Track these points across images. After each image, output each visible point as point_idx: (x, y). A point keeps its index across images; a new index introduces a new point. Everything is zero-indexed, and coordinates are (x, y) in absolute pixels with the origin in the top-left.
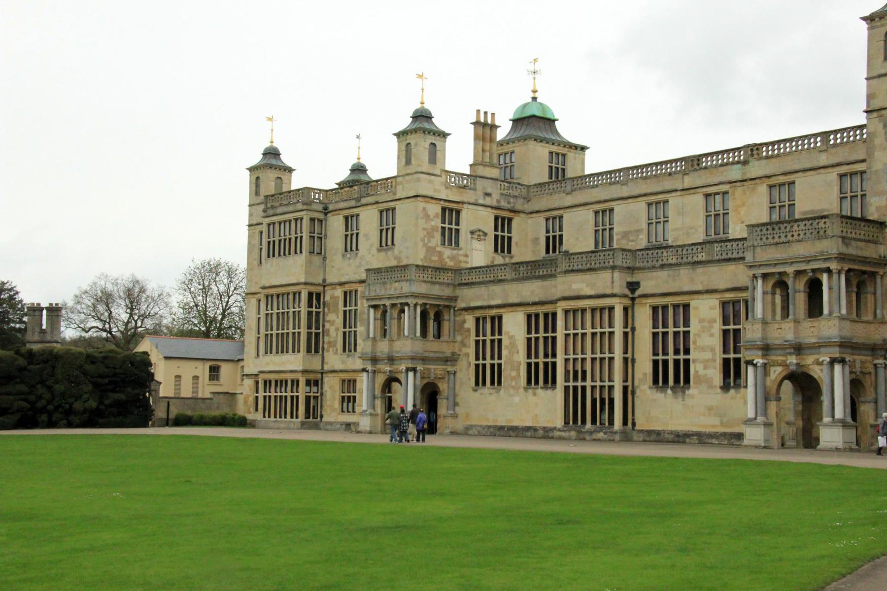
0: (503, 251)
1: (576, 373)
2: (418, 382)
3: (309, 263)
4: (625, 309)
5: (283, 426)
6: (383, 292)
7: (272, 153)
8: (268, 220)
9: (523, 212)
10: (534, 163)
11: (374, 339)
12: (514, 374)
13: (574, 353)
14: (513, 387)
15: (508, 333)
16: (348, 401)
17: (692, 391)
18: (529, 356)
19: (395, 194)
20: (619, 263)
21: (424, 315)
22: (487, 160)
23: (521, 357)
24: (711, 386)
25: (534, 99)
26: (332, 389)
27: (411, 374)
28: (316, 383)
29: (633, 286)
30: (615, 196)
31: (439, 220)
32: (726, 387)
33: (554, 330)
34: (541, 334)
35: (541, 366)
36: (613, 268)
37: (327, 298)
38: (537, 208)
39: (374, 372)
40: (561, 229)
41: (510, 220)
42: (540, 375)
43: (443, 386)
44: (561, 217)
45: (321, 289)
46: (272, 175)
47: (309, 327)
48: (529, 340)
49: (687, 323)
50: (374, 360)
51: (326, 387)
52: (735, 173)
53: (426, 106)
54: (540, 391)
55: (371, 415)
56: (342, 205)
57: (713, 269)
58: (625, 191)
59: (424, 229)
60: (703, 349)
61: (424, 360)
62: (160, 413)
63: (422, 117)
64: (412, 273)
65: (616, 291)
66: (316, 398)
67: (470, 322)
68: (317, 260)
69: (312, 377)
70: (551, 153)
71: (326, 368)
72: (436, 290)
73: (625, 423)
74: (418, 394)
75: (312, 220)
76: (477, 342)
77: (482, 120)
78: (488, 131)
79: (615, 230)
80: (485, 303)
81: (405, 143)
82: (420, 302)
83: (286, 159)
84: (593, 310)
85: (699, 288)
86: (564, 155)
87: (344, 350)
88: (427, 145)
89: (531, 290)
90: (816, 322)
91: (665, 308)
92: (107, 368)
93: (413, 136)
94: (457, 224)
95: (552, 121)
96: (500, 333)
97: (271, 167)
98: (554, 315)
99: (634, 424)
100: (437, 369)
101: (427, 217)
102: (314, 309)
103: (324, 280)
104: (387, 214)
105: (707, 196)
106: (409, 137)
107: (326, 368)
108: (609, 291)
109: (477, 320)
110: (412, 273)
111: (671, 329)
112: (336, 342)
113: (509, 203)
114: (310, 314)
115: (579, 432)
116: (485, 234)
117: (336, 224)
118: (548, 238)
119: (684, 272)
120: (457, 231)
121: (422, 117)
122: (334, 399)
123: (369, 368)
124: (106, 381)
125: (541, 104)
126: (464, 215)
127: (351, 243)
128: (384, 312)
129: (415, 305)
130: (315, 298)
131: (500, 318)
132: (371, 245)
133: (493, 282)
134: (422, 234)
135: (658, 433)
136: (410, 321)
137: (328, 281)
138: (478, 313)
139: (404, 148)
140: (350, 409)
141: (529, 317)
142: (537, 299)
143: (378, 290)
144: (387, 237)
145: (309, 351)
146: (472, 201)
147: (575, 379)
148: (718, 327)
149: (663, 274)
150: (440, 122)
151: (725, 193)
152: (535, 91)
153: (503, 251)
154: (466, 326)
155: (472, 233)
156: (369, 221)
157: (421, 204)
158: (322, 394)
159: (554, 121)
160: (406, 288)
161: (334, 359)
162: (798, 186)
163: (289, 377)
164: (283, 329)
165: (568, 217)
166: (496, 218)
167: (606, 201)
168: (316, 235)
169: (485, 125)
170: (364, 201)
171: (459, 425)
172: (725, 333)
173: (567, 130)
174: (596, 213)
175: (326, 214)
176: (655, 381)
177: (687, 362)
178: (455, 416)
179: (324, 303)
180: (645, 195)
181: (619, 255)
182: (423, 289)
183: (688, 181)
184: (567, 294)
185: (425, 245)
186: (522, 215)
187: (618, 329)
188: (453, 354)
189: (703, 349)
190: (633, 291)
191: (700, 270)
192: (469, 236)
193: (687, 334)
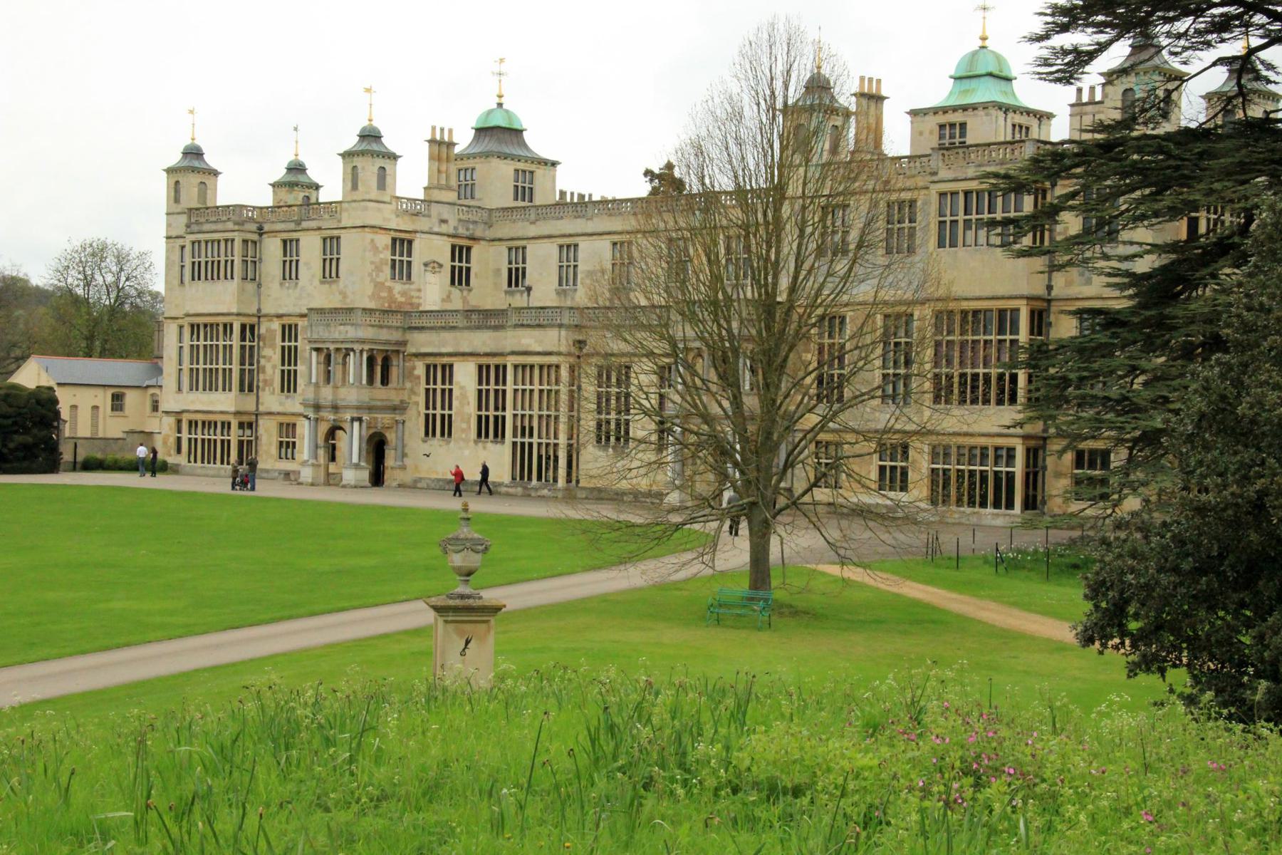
0: (460, 283)
1: (523, 428)
2: (364, 432)
3: (242, 291)
4: (572, 369)
5: (212, 472)
6: (325, 335)
7: (193, 153)
8: (193, 237)
9: (483, 239)
10: (496, 184)
11: (317, 385)
12: (464, 426)
13: (523, 409)
14: (463, 440)
15: (458, 383)
16: (287, 447)
18: (480, 409)
19: (340, 221)
20: (566, 321)
21: (371, 361)
22: (443, 182)
23: (472, 409)
25: (500, 105)
26: (268, 434)
27: (356, 424)
28: (250, 425)
29: (580, 344)
30: (579, 231)
31: (389, 252)
33: (504, 383)
35: (491, 420)
36: (560, 326)
37: (263, 331)
38: (499, 235)
39: (317, 420)
40: (524, 262)
41: (469, 249)
42: (489, 428)
43: (391, 436)
44: (524, 248)
45: (255, 320)
46: (195, 179)
47: (242, 363)
48: (480, 391)
50: (317, 407)
51: (261, 431)
53: (375, 124)
54: (490, 445)
55: (313, 465)
58: (590, 227)
59: (372, 263)
61: (371, 409)
62: (67, 456)
63: (370, 135)
64: (358, 317)
65: (563, 349)
66: (249, 442)
67: (420, 370)
68: (250, 287)
69: (245, 419)
70: (517, 171)
71: (262, 409)
72: (384, 335)
73: (569, 481)
74: (364, 445)
75: (245, 242)
76: (427, 390)
77: (438, 138)
78: (444, 149)
79: (580, 269)
80: (435, 350)
81: (351, 166)
82: (367, 347)
83: (211, 160)
84: (541, 367)
86: (532, 172)
87: (282, 391)
88: (375, 169)
89: (482, 341)
92: (11, 406)
93: (360, 158)
94: (410, 255)
96: (451, 383)
97: (194, 170)
98: (505, 367)
99: (578, 482)
100: (384, 419)
101: (375, 249)
102: (247, 343)
103: (259, 310)
104: (331, 244)
106: (355, 159)
107: (262, 409)
108: (555, 349)
109: (428, 367)
110: (358, 317)
112: (272, 380)
113: (468, 229)
114: (243, 347)
115: (525, 488)
116: (441, 266)
117: (272, 249)
118: (510, 270)
120: (409, 263)
121: (370, 135)
122: (271, 444)
123: (312, 415)
124: (10, 421)
125: (507, 111)
126: (416, 245)
127: (290, 270)
128: (328, 357)
129: (361, 351)
130: (249, 331)
131: (451, 366)
132: (313, 276)
133: (443, 328)
134: (370, 267)
136: (355, 367)
137: (264, 311)
138: (430, 360)
139: (349, 170)
140: (289, 455)
141: (480, 367)
142: (488, 350)
143: (321, 332)
144: (331, 268)
145: (242, 390)
146: (426, 229)
147: (523, 435)
150: (390, 142)
152: (500, 97)
153: (460, 283)
154: (416, 372)
155: (426, 265)
156: (310, 247)
157: (368, 235)
158: (257, 438)
159: (521, 131)
160: (351, 332)
161: (272, 400)
163: (220, 418)
165: (533, 250)
166: (453, 247)
167: (570, 236)
168: (249, 259)
169: (440, 143)
171: (407, 477)
173: (537, 143)
174: (561, 247)
175: (261, 235)
178: (403, 468)
179: (259, 336)
180: (609, 233)
181: (566, 314)
182: (369, 333)
184: (517, 349)
185: (372, 280)
186: (482, 243)
187: (564, 389)
188: (402, 402)
190: (581, 349)
192: (423, 268)
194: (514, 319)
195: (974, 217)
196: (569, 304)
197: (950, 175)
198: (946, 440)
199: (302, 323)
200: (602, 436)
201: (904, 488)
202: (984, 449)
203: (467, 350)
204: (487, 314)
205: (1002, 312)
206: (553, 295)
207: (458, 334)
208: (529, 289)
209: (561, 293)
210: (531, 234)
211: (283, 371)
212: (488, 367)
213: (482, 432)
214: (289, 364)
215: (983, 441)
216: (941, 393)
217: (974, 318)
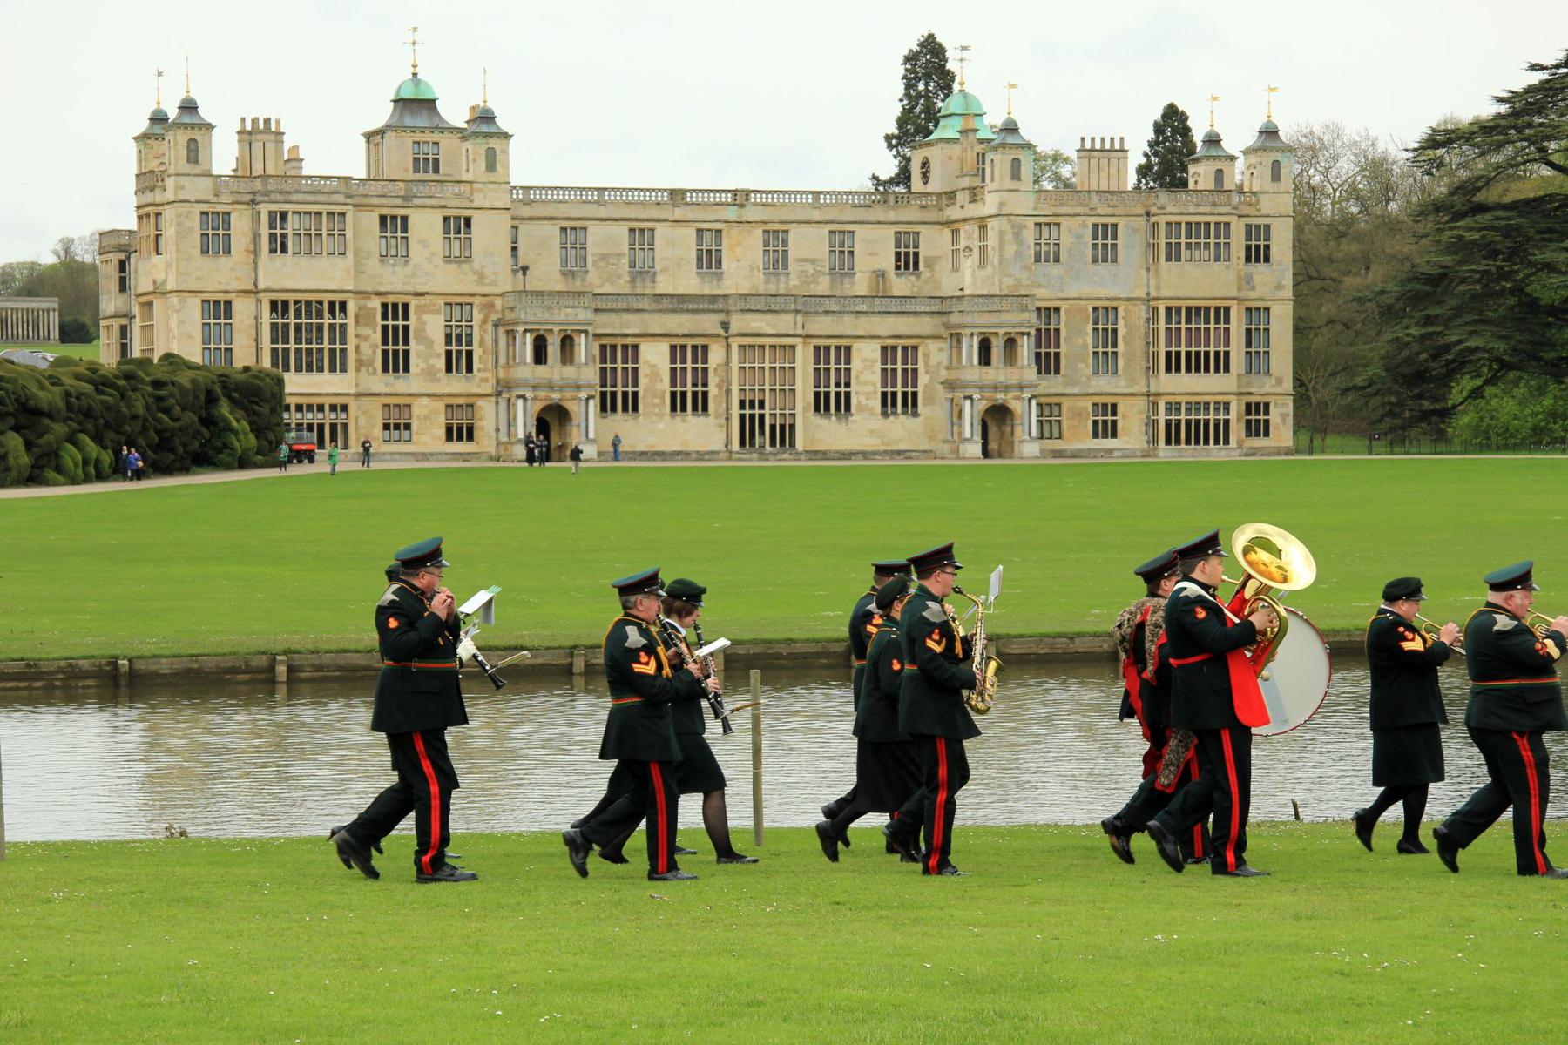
6: (547, 316)
12: (657, 401)
15: (646, 362)
17: (856, 417)
24: (872, 414)
25: (415, 75)
32: (885, 414)
34: (689, 365)
36: (797, 311)
42: (689, 400)
48: (673, 370)
49: (848, 362)
52: (731, 213)
56: (375, 201)
57: (876, 319)
60: (865, 383)
84: (773, 347)
85: (862, 333)
87: (385, 369)
88: (483, 152)
90: (985, 369)
91: (827, 348)
95: (430, 104)
105: (699, 230)
110: (586, 301)
111: (833, 366)
119: (847, 319)
133: (627, 310)
135: (824, 453)
138: (606, 341)
141: (673, 347)
148: (878, 366)
149: (828, 319)
151: (720, 231)
162: (791, 235)
164: (309, 341)
170: (416, 201)
172: (884, 371)
176: (817, 409)
177: (848, 395)
183: (679, 213)
189: (865, 383)
191: (863, 319)
193: (848, 371)
194: (741, 305)
195: (1193, 241)
196: (577, 285)
197: (1175, 210)
198: (1179, 399)
199: (413, 303)
200: (821, 404)
201: (1114, 435)
202: (1207, 405)
203: (658, 331)
204: (682, 298)
205: (1217, 309)
206: (558, 276)
207: (646, 316)
208: (525, 269)
209: (567, 274)
210: (526, 215)
211: (385, 353)
212: (684, 347)
213: (677, 403)
214: (396, 342)
215: (1207, 398)
216: (1173, 363)
217: (1193, 312)
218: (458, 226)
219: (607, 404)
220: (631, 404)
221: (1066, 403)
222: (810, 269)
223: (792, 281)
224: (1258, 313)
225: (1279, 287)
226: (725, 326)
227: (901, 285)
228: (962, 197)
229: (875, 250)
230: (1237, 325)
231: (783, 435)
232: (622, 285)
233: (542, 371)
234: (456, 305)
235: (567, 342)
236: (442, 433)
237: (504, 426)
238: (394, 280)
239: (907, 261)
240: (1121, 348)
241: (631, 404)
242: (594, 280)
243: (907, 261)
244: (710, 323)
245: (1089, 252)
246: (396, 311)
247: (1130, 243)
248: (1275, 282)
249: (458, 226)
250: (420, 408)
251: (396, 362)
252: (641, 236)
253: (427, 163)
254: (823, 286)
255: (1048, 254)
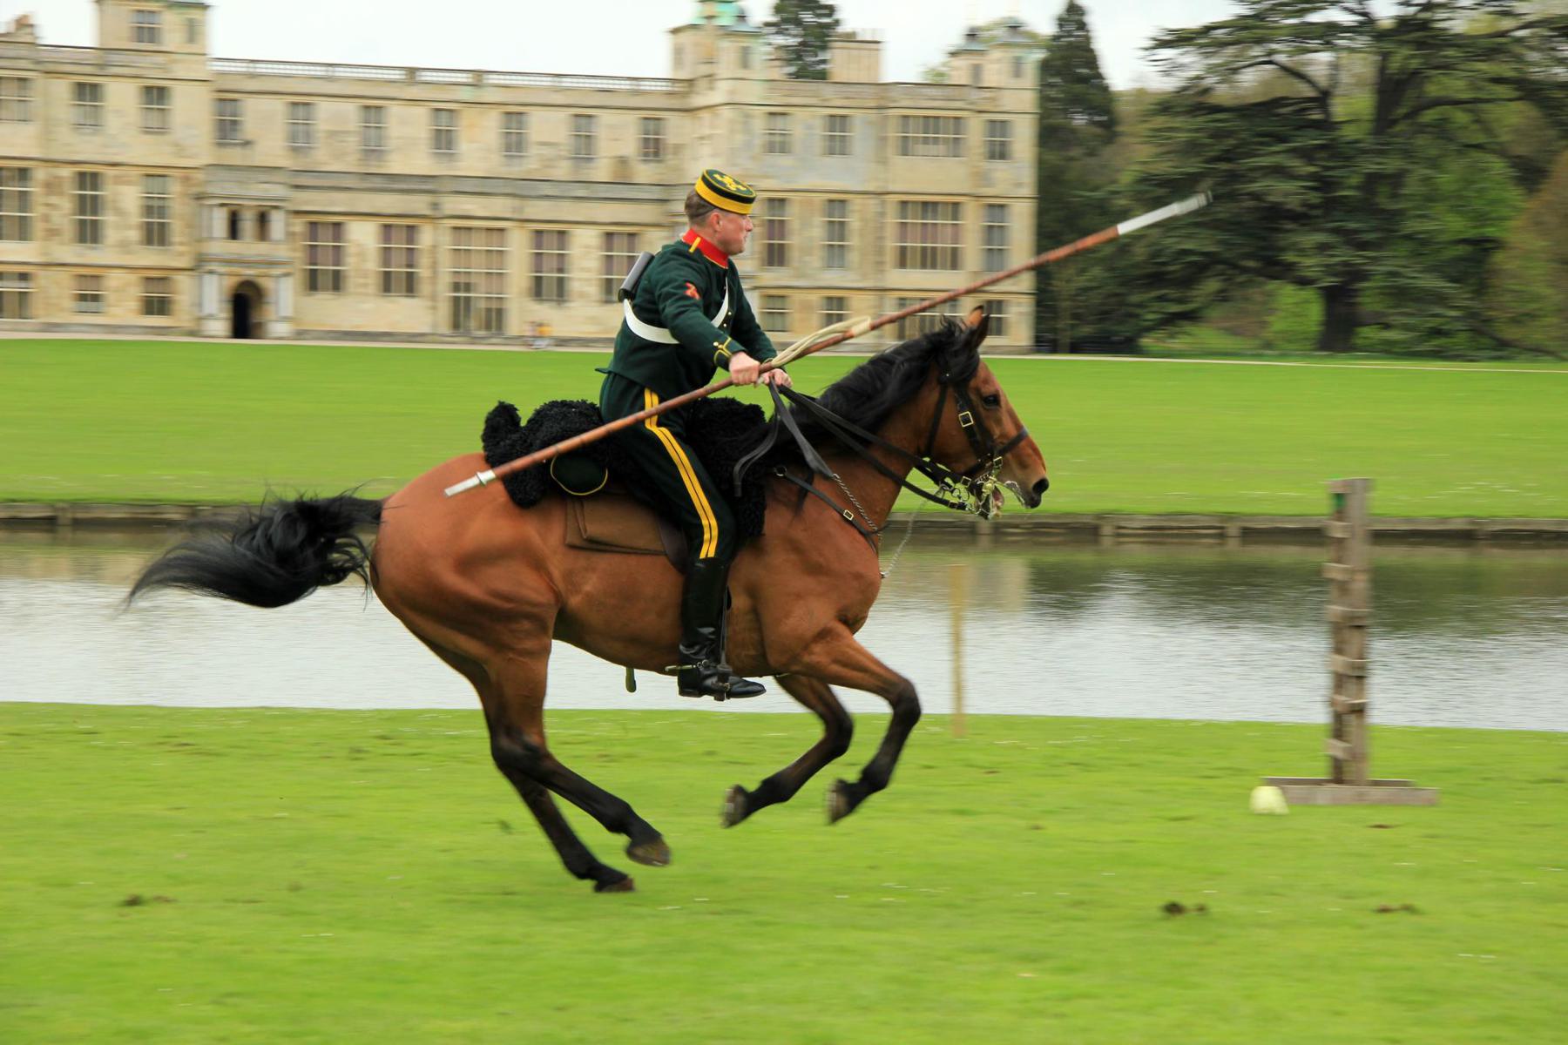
42: (399, 281)
52: (466, 94)
60: (583, 269)
67: (299, 225)
119: (566, 204)
189: (583, 269)
200: (538, 289)
216: (903, 260)
217: (928, 207)
218: (156, 95)
219: (313, 282)
220: (337, 283)
221: (797, 296)
222: (546, 151)
223: (529, 165)
224: (997, 209)
225: (1019, 185)
226: (435, 206)
227: (645, 172)
228: (702, 84)
229: (618, 137)
230: (973, 221)
231: (495, 319)
232: (350, 163)
233: (234, 248)
234: (155, 175)
235: (263, 219)
236: (134, 305)
237: (208, 301)
238: (87, 148)
239: (653, 148)
240: (853, 241)
241: (337, 283)
242: (323, 158)
243: (653, 148)
244: (419, 204)
245: (819, 145)
246: (88, 179)
247: (860, 133)
248: (1016, 178)
249: (156, 95)
250: (114, 279)
251: (89, 233)
252: (373, 111)
253: (147, 33)
254: (563, 171)
255: (778, 145)
